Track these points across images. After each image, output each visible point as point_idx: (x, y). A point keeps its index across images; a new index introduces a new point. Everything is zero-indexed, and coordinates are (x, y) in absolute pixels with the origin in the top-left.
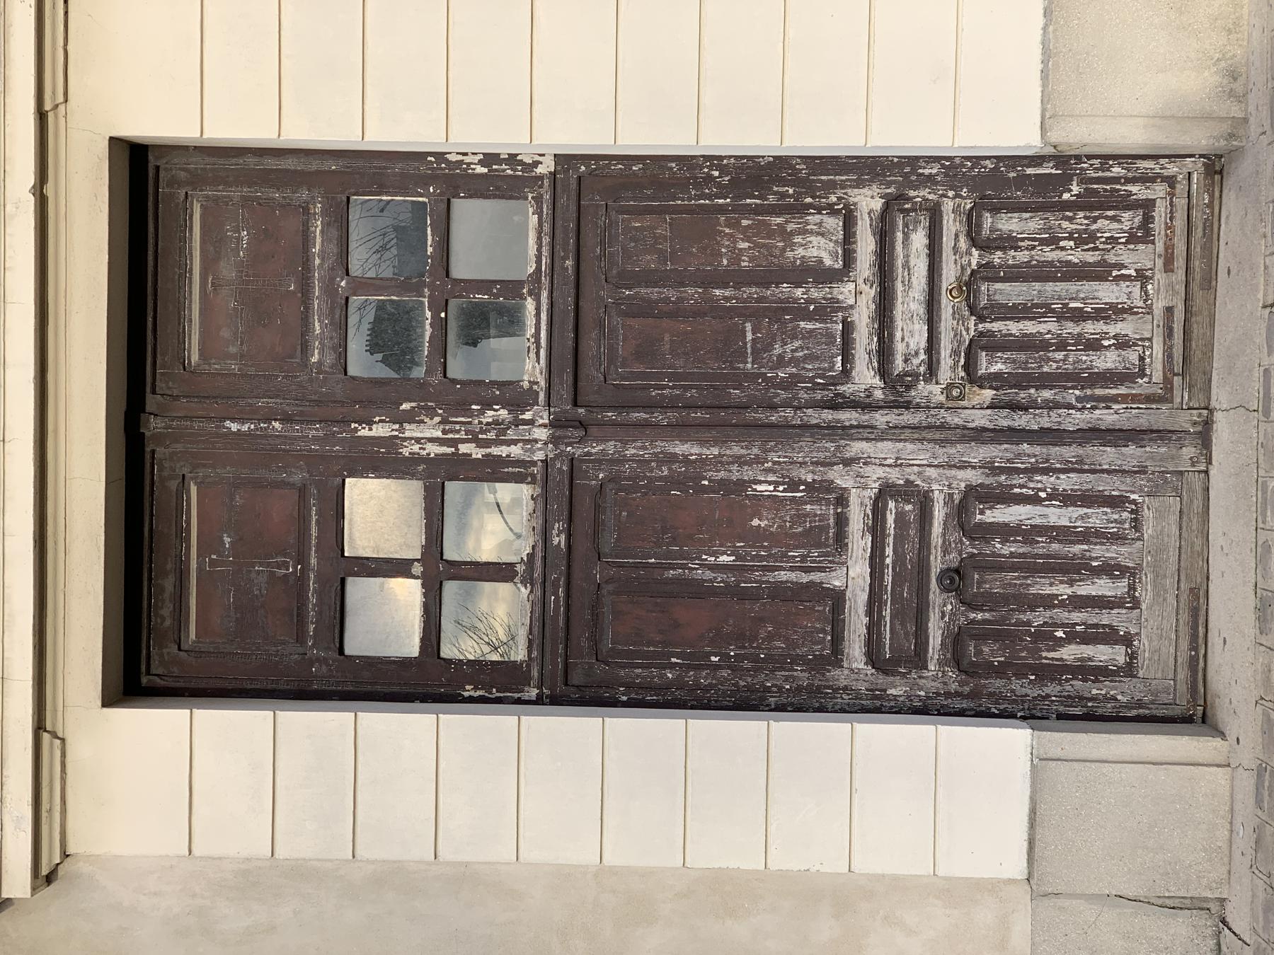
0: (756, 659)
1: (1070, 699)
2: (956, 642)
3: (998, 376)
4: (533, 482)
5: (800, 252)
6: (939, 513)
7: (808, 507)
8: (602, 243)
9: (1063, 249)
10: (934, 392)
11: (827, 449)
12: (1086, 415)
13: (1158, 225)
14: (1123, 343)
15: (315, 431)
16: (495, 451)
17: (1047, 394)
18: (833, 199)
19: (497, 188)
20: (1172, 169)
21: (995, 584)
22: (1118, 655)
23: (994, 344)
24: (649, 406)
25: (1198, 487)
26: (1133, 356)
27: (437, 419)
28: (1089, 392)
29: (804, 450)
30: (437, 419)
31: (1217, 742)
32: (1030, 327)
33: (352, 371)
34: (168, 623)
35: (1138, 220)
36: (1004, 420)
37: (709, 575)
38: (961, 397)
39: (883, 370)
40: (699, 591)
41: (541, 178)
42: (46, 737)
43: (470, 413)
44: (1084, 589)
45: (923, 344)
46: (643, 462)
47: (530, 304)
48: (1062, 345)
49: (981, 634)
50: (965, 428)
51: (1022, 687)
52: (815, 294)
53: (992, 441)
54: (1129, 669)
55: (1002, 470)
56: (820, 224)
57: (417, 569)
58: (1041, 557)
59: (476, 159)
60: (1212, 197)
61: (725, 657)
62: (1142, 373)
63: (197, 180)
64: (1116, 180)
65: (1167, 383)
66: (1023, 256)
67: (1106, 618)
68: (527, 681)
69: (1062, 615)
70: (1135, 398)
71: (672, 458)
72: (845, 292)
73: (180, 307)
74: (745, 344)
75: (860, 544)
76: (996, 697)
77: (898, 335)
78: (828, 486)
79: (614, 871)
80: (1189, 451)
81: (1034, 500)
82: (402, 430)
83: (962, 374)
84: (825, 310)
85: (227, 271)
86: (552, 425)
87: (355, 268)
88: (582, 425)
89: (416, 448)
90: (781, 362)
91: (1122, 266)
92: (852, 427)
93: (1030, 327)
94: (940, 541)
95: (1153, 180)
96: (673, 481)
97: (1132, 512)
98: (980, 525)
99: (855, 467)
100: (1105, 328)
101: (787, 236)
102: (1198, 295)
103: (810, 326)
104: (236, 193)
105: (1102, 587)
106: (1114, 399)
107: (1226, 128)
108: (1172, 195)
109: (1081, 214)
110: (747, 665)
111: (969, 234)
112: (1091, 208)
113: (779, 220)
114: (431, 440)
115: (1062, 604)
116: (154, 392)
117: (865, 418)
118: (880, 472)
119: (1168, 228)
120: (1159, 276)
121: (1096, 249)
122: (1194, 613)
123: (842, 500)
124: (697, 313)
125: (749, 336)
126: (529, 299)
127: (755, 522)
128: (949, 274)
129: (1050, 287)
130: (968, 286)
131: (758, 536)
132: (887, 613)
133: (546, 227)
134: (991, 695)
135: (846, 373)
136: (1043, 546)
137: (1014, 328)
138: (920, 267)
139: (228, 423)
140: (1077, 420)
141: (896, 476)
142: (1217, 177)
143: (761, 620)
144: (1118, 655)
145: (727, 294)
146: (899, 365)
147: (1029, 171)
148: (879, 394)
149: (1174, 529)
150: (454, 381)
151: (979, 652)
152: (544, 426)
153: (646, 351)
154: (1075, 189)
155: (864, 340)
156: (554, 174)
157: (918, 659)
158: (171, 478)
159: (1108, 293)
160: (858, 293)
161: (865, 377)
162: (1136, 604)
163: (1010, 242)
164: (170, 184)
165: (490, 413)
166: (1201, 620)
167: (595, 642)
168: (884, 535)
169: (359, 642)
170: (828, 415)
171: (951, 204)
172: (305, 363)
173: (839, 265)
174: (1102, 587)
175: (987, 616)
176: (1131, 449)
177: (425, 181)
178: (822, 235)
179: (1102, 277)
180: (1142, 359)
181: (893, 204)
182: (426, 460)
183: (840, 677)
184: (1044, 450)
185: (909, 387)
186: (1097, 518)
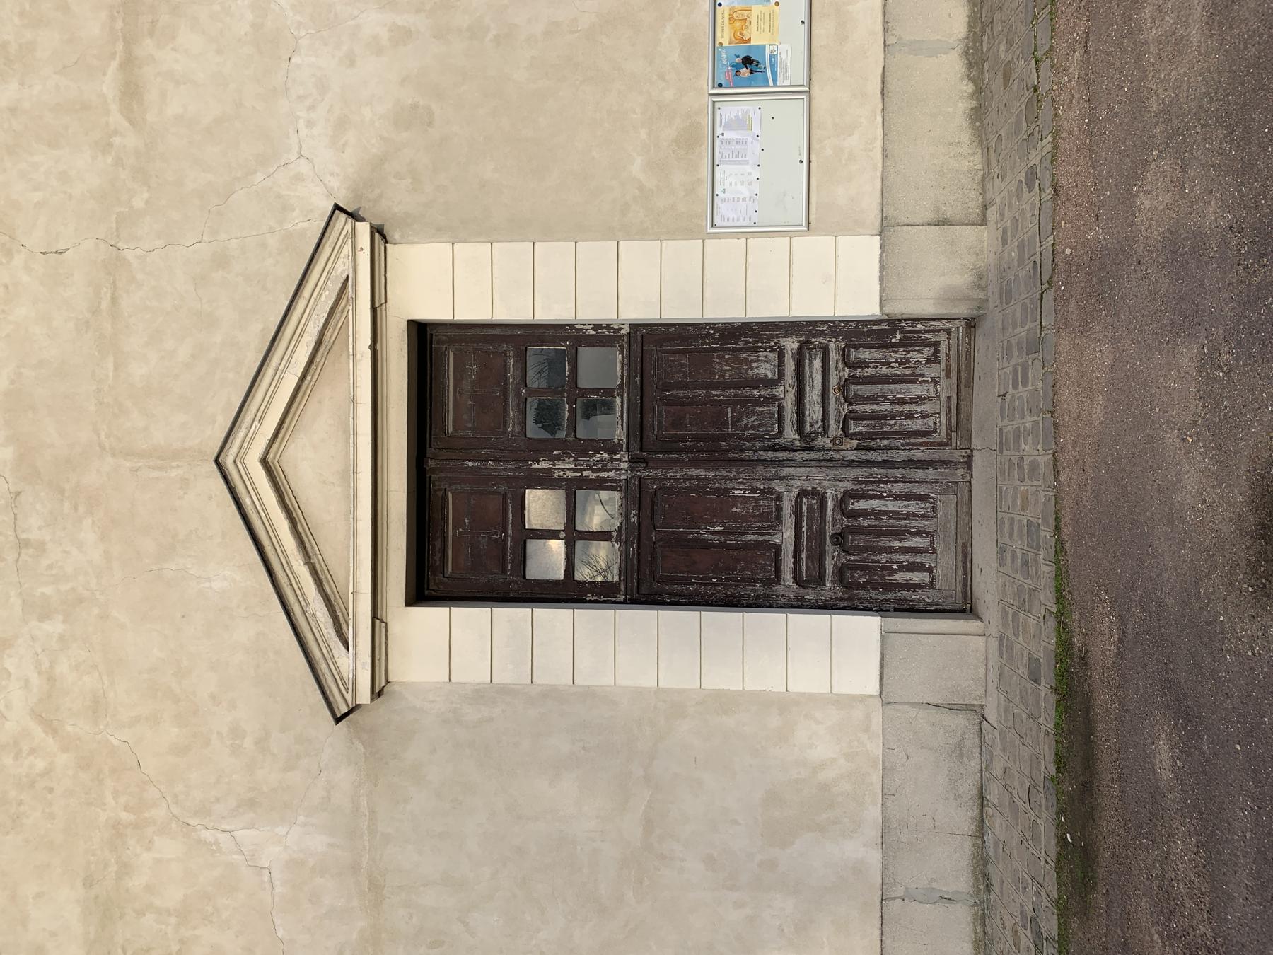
0: (736, 580)
2: (840, 571)
3: (860, 433)
4: (621, 490)
5: (756, 371)
6: (830, 504)
7: (762, 502)
8: (654, 368)
9: (893, 367)
11: (771, 472)
12: (907, 453)
13: (942, 355)
14: (925, 416)
15: (511, 465)
16: (601, 474)
17: (886, 442)
18: (773, 343)
19: (600, 342)
20: (949, 325)
21: (860, 541)
23: (857, 417)
24: (680, 451)
25: (966, 490)
26: (930, 423)
27: (572, 459)
28: (908, 441)
29: (759, 473)
30: (572, 459)
31: (979, 623)
32: (876, 408)
33: (529, 435)
34: (438, 563)
35: (931, 352)
36: (864, 456)
37: (711, 537)
38: (841, 444)
39: (800, 431)
40: (706, 545)
41: (623, 336)
42: (378, 621)
43: (587, 455)
44: (907, 544)
45: (820, 417)
46: (676, 480)
47: (618, 400)
48: (893, 417)
49: (854, 567)
50: (843, 460)
51: (876, 595)
52: (763, 392)
53: (858, 467)
54: (931, 585)
55: (863, 482)
56: (766, 357)
57: (562, 535)
58: (883, 526)
59: (590, 327)
60: (970, 340)
61: (720, 579)
62: (935, 431)
63: (451, 341)
64: (919, 332)
65: (949, 436)
66: (872, 371)
67: (919, 558)
68: (618, 591)
69: (896, 557)
70: (932, 444)
71: (691, 478)
72: (779, 391)
73: (443, 404)
74: (728, 418)
75: (788, 520)
76: (862, 600)
77: (807, 413)
78: (771, 491)
79: (665, 691)
80: (961, 471)
81: (881, 497)
82: (554, 465)
83: (841, 432)
84: (769, 401)
85: (466, 385)
86: (630, 461)
88: (645, 461)
89: (561, 473)
90: (746, 427)
91: (924, 376)
92: (784, 460)
93: (876, 408)
94: (831, 519)
95: (939, 331)
96: (692, 489)
97: (931, 503)
98: (852, 510)
99: (785, 481)
100: (915, 408)
101: (749, 363)
103: (761, 409)
104: (470, 347)
106: (921, 445)
107: (976, 304)
108: (949, 339)
109: (902, 349)
110: (731, 583)
111: (843, 360)
112: (907, 346)
113: (745, 355)
114: (569, 469)
115: (896, 551)
116: (430, 447)
117: (791, 455)
118: (799, 483)
119: (947, 356)
120: (943, 381)
121: (910, 367)
122: (965, 555)
123: (779, 498)
125: (730, 415)
126: (618, 398)
127: (734, 510)
128: (834, 381)
129: (886, 387)
130: (844, 387)
131: (735, 517)
132: (804, 556)
133: (626, 361)
134: (859, 599)
135: (780, 433)
136: (885, 521)
139: (467, 462)
140: (901, 455)
141: (807, 486)
142: (972, 329)
143: (737, 560)
145: (718, 393)
146: (808, 428)
147: (874, 328)
148: (797, 443)
149: (954, 512)
150: (580, 440)
151: (852, 577)
152: (626, 461)
154: (898, 336)
155: (789, 415)
156: (629, 334)
157: (821, 580)
158: (440, 490)
159: (917, 390)
160: (786, 392)
161: (790, 435)
162: (934, 551)
163: (864, 364)
164: (438, 343)
165: (599, 455)
166: (969, 559)
167: (653, 572)
168: (801, 516)
169: (533, 572)
170: (771, 454)
171: (834, 345)
172: (505, 432)
173: (776, 377)
175: (857, 557)
176: (930, 470)
177: (565, 339)
178: (767, 362)
180: (935, 424)
182: (567, 480)
183: (779, 589)
184: (885, 471)
185: (813, 440)
186: (913, 506)
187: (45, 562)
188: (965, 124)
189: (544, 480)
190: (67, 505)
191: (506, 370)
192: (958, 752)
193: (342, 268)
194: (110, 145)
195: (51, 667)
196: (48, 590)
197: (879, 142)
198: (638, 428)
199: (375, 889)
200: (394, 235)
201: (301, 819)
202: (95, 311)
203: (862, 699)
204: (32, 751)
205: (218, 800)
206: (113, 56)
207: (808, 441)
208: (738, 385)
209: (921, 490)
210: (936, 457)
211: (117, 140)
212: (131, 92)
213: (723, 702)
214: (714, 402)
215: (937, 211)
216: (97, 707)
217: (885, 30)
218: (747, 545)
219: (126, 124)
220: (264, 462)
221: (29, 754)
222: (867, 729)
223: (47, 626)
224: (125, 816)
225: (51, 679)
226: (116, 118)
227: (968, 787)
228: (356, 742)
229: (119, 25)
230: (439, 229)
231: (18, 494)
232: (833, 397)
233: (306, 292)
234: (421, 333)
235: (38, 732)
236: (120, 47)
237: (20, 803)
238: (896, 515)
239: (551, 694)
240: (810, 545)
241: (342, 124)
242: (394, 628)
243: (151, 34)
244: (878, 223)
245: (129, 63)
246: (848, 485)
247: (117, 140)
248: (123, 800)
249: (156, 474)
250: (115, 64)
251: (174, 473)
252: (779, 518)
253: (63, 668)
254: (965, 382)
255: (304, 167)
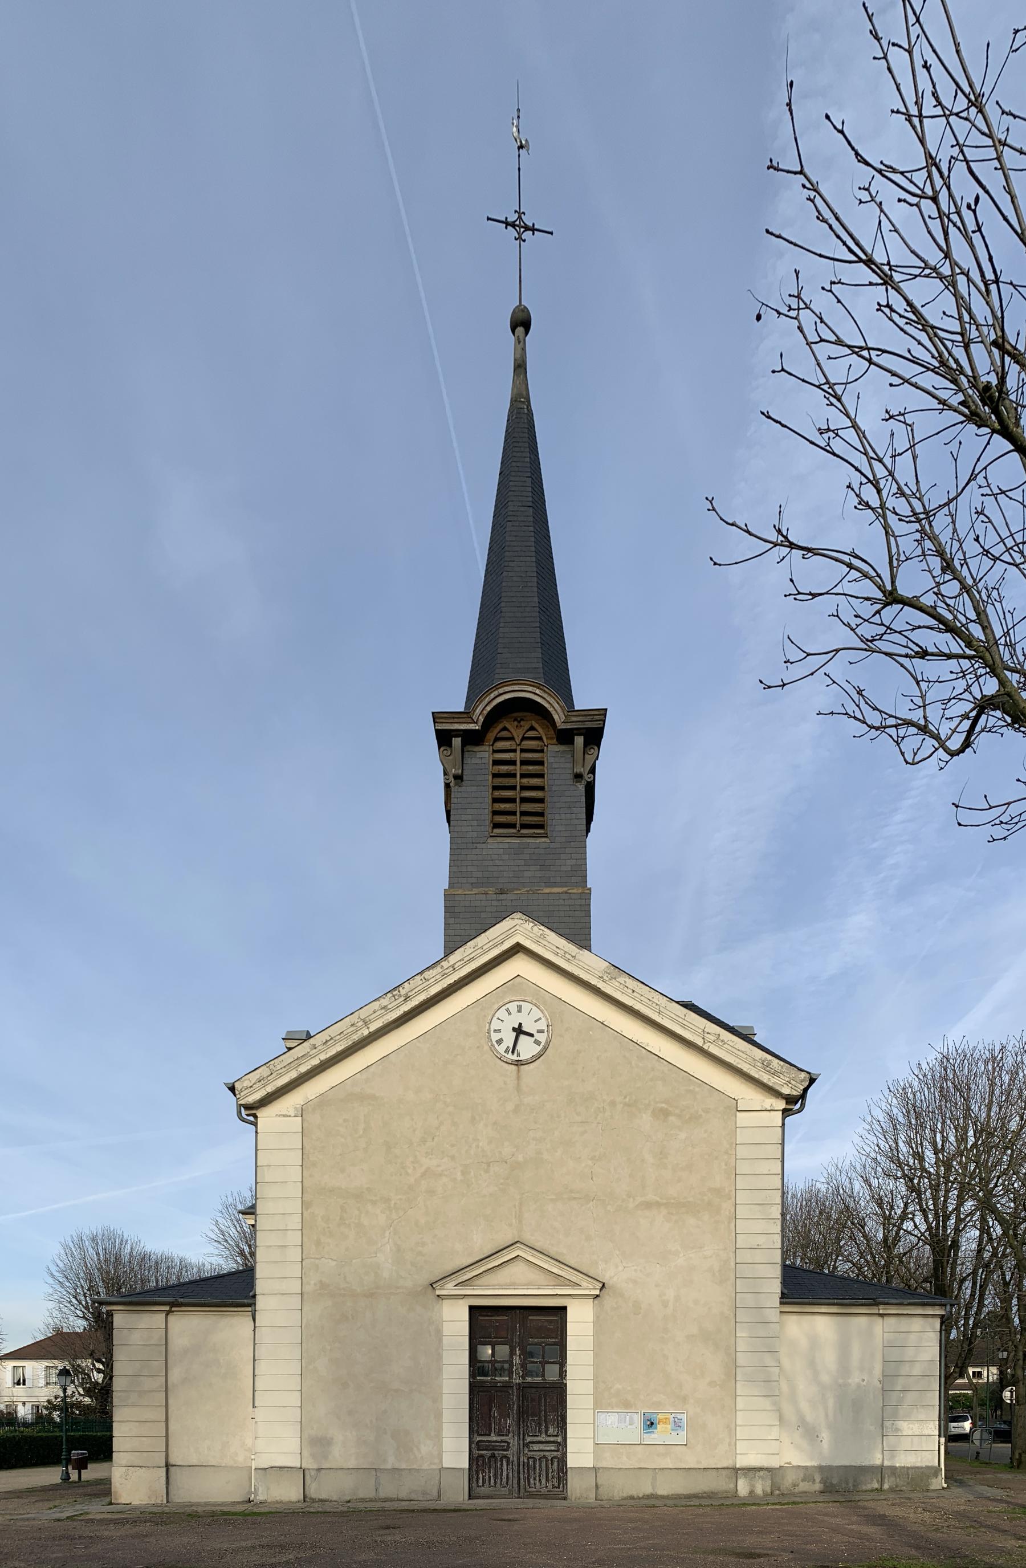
1: (473, 1475)
2: (482, 1456)
6: (505, 1453)
10: (526, 1450)
14: (535, 1484)
15: (517, 1340)
22: (481, 1484)
24: (523, 1401)
26: (533, 1486)
29: (515, 1428)
32: (538, 1468)
39: (529, 1442)
40: (490, 1410)
44: (492, 1478)
48: (534, 1473)
51: (474, 1468)
54: (478, 1486)
63: (561, 1318)
65: (528, 1492)
67: (487, 1482)
68: (474, 1379)
69: (487, 1474)
75: (499, 1439)
78: (509, 1433)
79: (442, 1396)
80: (516, 1495)
84: (540, 1431)
85: (546, 1324)
87: (547, 1347)
90: (531, 1424)
93: (538, 1468)
101: (553, 1425)
102: (543, 1496)
104: (559, 1325)
105: (492, 1481)
123: (507, 1435)
124: (539, 1409)
128: (547, 1454)
130: (545, 1457)
135: (529, 1436)
137: (537, 1465)
138: (548, 1449)
140: (522, 1476)
141: (511, 1445)
144: (481, 1484)
146: (531, 1445)
153: (533, 1400)
157: (479, 1450)
159: (544, 1481)
161: (529, 1439)
163: (552, 1464)
164: (561, 1314)
167: (481, 1391)
169: (480, 1348)
170: (522, 1432)
172: (529, 1338)
174: (492, 1481)
179: (546, 1480)
181: (559, 1443)
186: (504, 1480)
187: (482, 1173)
188: (629, 1495)
189: (512, 1353)
190: (502, 1181)
191: (551, 1338)
192: (424, 1493)
193: (584, 1284)
194: (630, 1197)
195: (445, 1175)
196: (472, 1173)
197: (623, 1467)
198: (531, 1386)
199: (370, 1295)
200: (596, 1302)
201: (394, 1268)
202: (571, 1191)
203: (441, 1462)
204: (414, 1168)
205: (400, 1238)
206: (661, 1199)
207: (527, 1445)
208: (545, 1421)
209: (510, 1483)
210: (521, 1488)
211: (631, 1200)
212: (648, 1205)
213: (439, 1416)
214: (540, 1412)
215: (601, 1485)
216: (431, 1192)
217: (660, 1469)
218: (490, 1424)
219: (637, 1203)
220: (518, 1256)
221: (414, 1167)
222: (431, 1464)
223: (459, 1174)
224: (393, 1202)
225: (441, 1175)
226: (639, 1199)
227: (413, 1496)
228: (421, 1288)
229: (672, 1201)
230: (598, 1317)
231: (506, 1162)
232: (542, 1454)
233: (575, 1272)
234: (565, 1308)
235: (423, 1169)
236: (664, 1201)
237: (396, 1164)
238: (502, 1474)
239: (440, 1357)
240: (491, 1447)
241: (635, 1282)
242: (461, 1302)
243: (669, 1213)
244: (597, 1466)
245: (658, 1205)
246: (511, 1459)
247: (631, 1200)
248: (398, 1202)
249: (514, 1214)
250: (658, 1199)
251: (514, 1221)
252: (500, 1435)
253: (444, 1179)
254: (545, 1497)
255: (621, 1268)
